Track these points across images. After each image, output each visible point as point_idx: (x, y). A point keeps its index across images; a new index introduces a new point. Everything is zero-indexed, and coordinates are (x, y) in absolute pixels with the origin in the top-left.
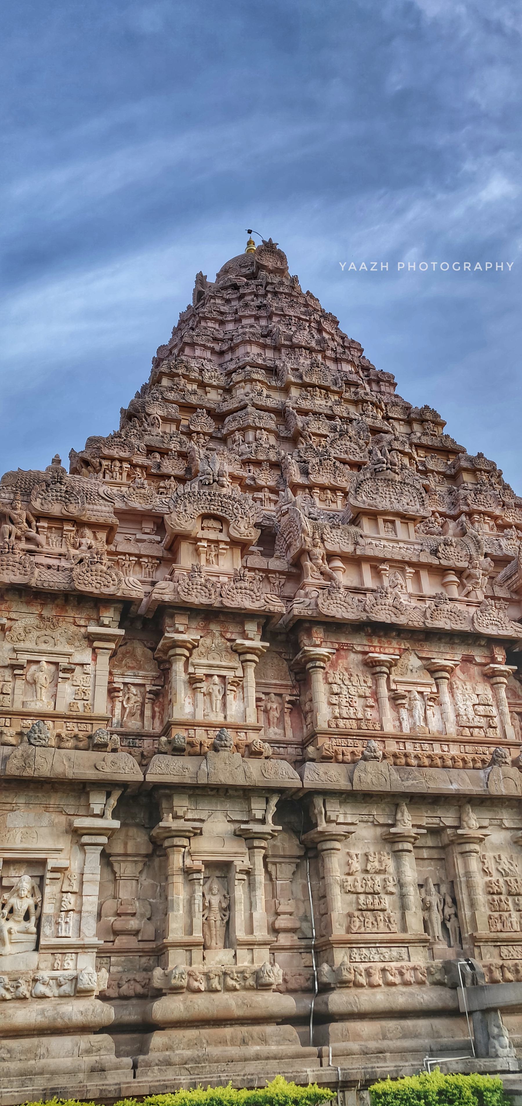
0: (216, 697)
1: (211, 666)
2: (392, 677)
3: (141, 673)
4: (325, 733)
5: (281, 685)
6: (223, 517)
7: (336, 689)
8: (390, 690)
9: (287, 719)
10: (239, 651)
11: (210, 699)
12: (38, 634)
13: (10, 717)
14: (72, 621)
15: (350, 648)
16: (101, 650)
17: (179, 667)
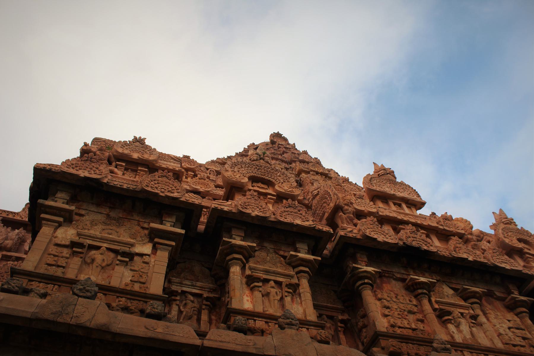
0: (274, 297)
1: (267, 272)
2: (433, 299)
3: (199, 284)
4: (386, 336)
5: (332, 308)
6: (269, 181)
7: (386, 303)
8: (435, 310)
9: (342, 336)
10: (293, 264)
11: (269, 300)
12: (104, 227)
13: (60, 284)
14: (136, 223)
15: (391, 275)
16: (161, 246)
17: (235, 270)
